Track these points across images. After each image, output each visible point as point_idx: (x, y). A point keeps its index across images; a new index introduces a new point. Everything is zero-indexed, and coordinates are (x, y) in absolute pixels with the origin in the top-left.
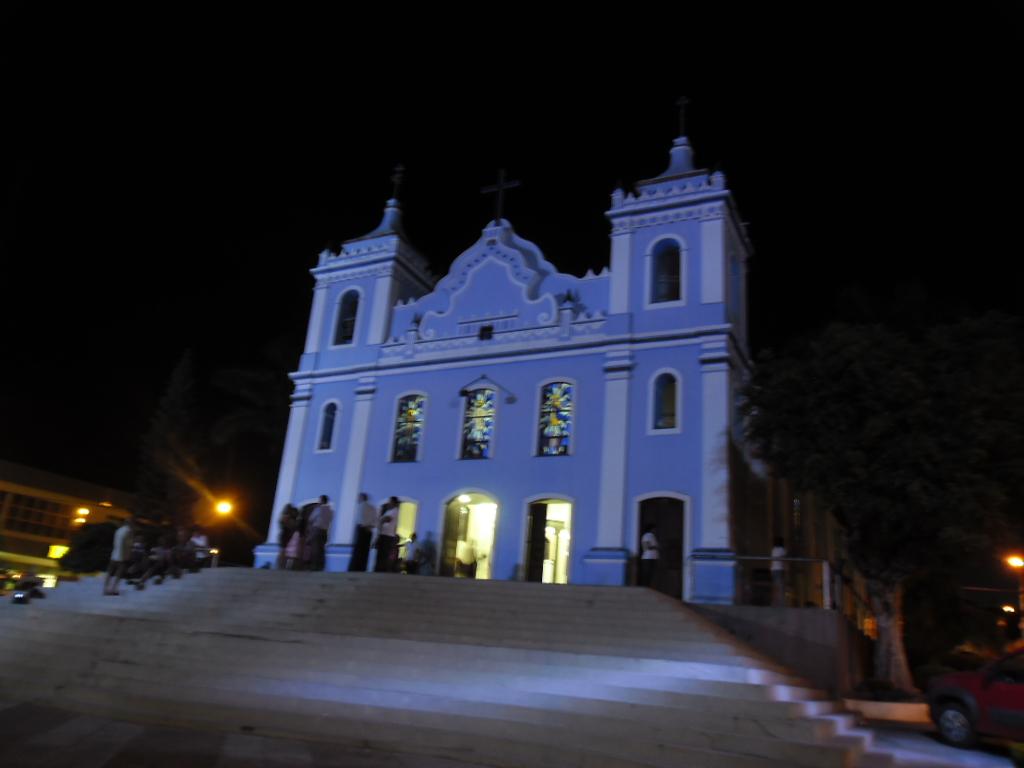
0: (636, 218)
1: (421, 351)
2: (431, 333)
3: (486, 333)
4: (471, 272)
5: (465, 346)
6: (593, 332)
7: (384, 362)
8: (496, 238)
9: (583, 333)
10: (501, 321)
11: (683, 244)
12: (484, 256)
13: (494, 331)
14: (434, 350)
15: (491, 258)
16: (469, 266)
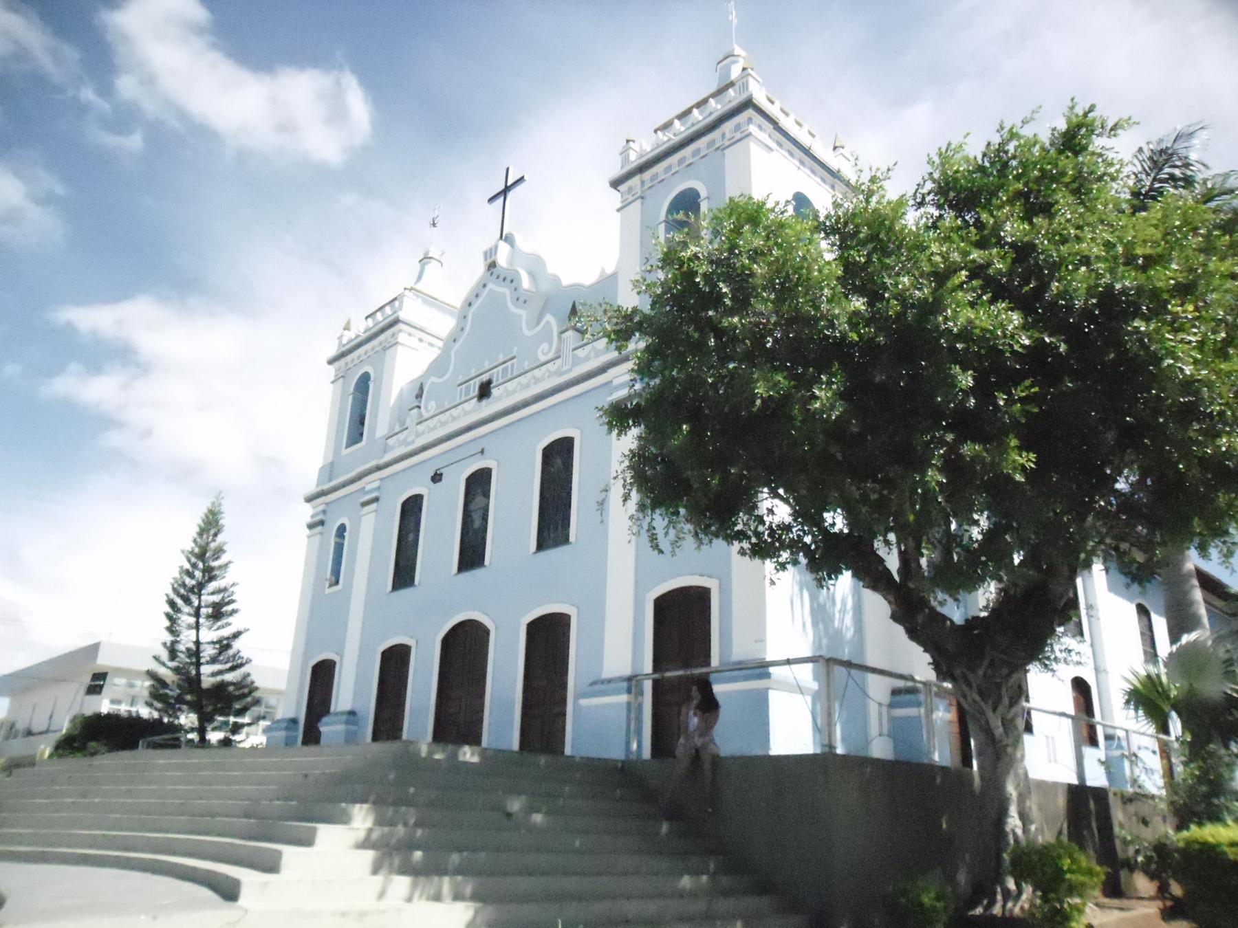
0: (647, 175)
3: (485, 391)
5: (466, 413)
9: (587, 359)
10: (500, 368)
11: (703, 193)
14: (435, 428)
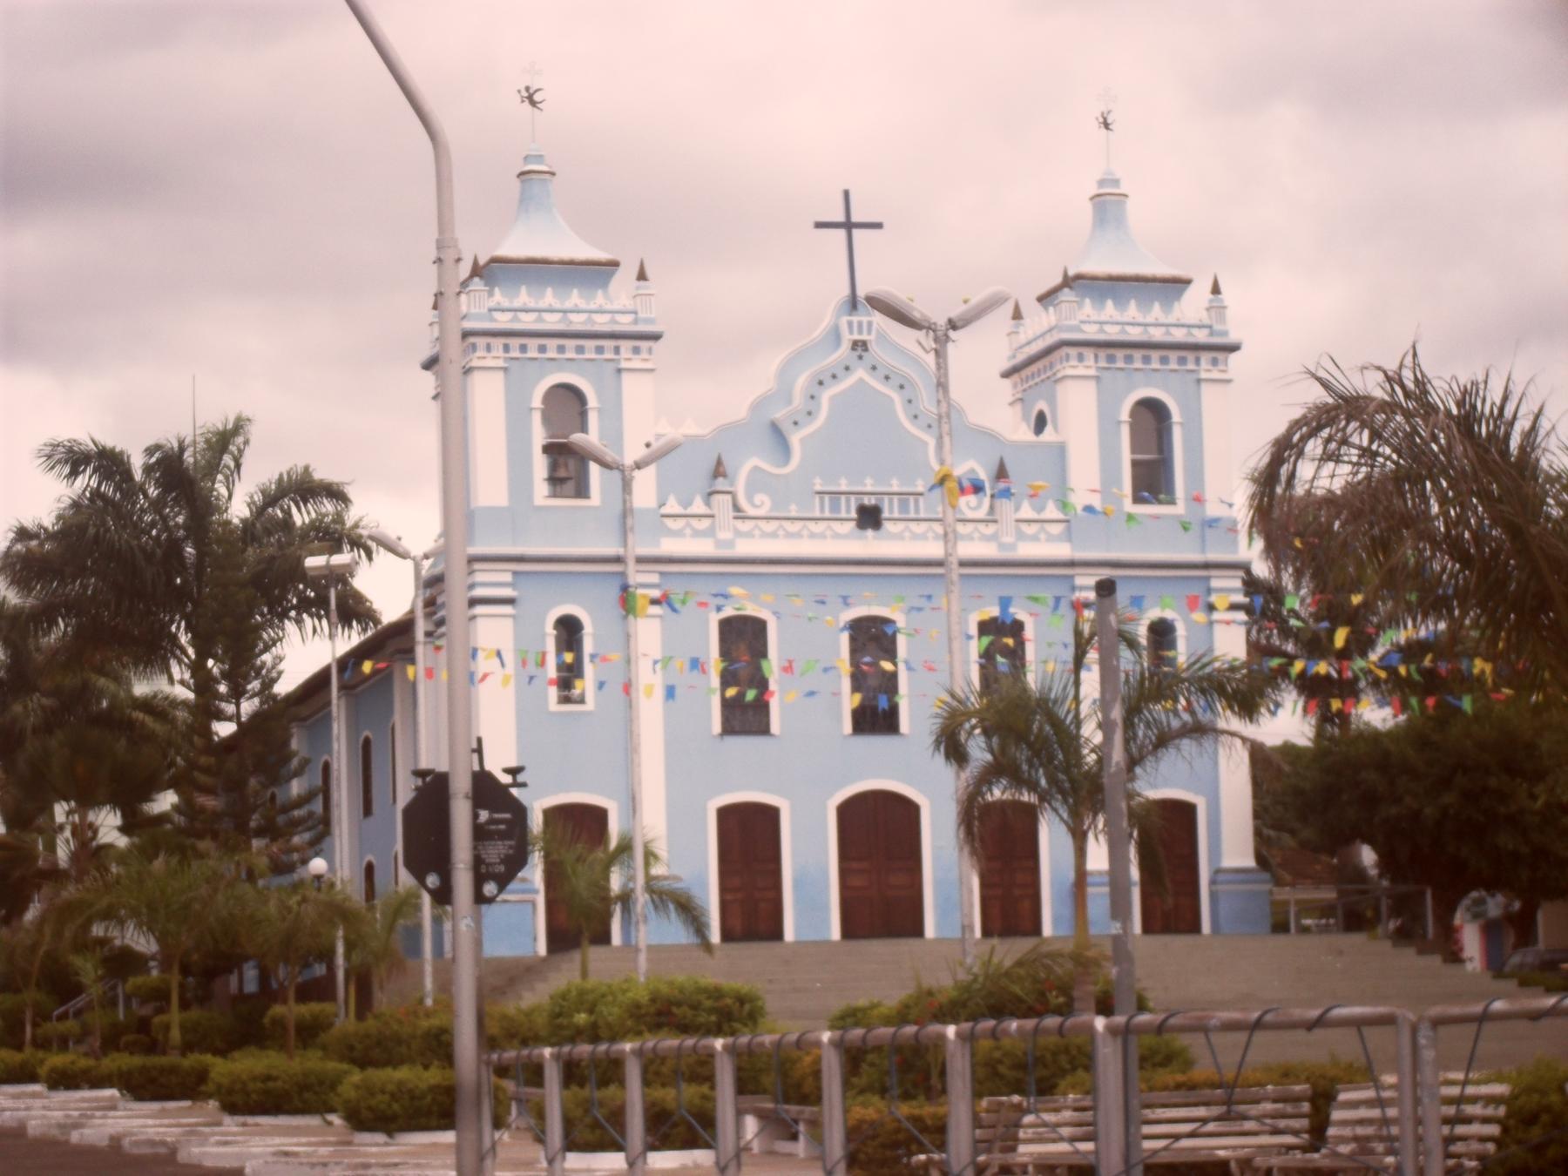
1: (749, 535)
2: (762, 504)
3: (870, 517)
4: (826, 396)
5: (837, 536)
6: (1051, 538)
7: (669, 547)
8: (864, 337)
9: (1035, 538)
11: (1176, 416)
12: (847, 368)
13: (886, 514)
14: (774, 535)
15: (860, 373)
16: (821, 383)
